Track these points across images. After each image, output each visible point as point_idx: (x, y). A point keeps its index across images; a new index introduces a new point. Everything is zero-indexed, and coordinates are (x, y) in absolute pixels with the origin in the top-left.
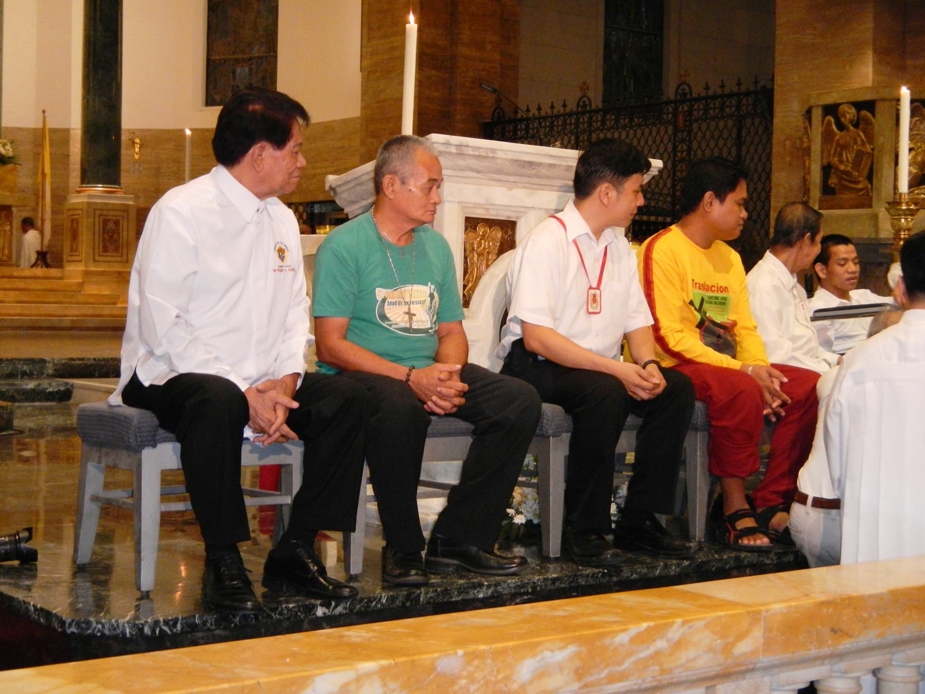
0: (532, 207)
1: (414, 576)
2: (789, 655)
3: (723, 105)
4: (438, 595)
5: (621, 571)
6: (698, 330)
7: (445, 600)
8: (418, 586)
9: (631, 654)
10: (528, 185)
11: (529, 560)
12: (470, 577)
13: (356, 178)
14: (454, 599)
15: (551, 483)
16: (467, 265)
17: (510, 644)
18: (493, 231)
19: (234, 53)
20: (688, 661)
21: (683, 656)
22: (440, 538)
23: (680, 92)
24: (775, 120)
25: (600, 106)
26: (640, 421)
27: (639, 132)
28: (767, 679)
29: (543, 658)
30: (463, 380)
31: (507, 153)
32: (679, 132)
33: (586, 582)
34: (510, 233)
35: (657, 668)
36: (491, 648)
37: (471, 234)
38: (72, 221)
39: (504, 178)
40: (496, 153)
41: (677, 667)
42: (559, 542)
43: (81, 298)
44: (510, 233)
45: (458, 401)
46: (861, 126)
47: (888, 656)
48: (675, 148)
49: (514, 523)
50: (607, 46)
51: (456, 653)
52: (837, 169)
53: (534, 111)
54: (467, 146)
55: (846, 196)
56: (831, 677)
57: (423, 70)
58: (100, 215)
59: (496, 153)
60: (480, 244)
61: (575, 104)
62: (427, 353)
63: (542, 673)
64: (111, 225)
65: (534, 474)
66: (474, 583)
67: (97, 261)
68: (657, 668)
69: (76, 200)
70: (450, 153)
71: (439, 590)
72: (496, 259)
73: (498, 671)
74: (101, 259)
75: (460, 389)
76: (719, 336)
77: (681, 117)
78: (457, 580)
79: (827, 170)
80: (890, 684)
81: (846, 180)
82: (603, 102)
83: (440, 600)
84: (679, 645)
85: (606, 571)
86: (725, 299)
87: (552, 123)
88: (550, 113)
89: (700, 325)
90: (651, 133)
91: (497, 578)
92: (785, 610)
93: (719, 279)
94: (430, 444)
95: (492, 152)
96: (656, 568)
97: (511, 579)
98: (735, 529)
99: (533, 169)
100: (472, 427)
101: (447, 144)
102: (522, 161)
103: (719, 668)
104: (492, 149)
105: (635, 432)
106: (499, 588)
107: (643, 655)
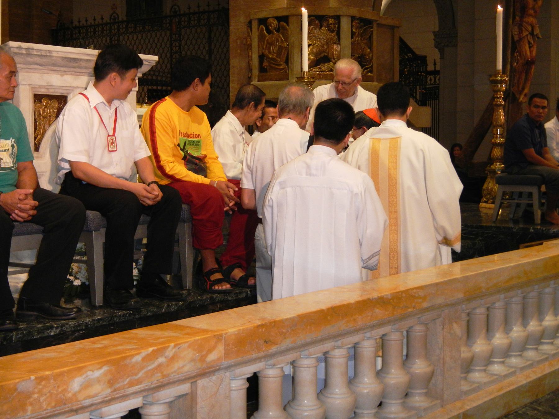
0: (77, 87)
1: (8, 325)
2: (240, 359)
4: (24, 336)
5: (141, 311)
6: (183, 161)
7: (29, 338)
8: (11, 331)
9: (143, 368)
10: (74, 73)
11: (83, 309)
12: (45, 322)
14: (35, 338)
15: (95, 260)
17: (65, 369)
18: (52, 102)
20: (179, 368)
21: (176, 366)
22: (24, 299)
23: (173, 10)
24: (231, 28)
25: (125, 19)
26: (148, 218)
27: (149, 35)
28: (227, 374)
29: (87, 376)
30: (34, 200)
33: (119, 319)
35: (158, 376)
36: (53, 373)
37: (38, 105)
39: (58, 69)
40: (52, 53)
41: (172, 373)
42: (102, 296)
45: (31, 212)
46: (281, 31)
47: (298, 353)
48: (171, 45)
49: (74, 285)
51: (30, 378)
52: (268, 57)
53: (83, 22)
54: (33, 49)
55: (273, 73)
56: (266, 368)
59: (52, 53)
60: (44, 111)
62: (11, 182)
63: (87, 385)
65: (84, 254)
66: (48, 326)
68: (159, 374)
70: (22, 54)
71: (25, 332)
72: (55, 120)
73: (58, 387)
75: (33, 205)
76: (196, 164)
77: (174, 26)
78: (36, 325)
79: (262, 57)
80: (300, 368)
81: (274, 64)
82: (127, 16)
83: (25, 338)
84: (173, 359)
85: (131, 312)
86: (199, 142)
87: (95, 29)
89: (184, 158)
91: (62, 322)
92: (236, 333)
93: (194, 129)
94: (15, 241)
95: (49, 53)
96: (162, 308)
97: (70, 321)
98: (210, 280)
100: (41, 228)
101: (20, 48)
103: (198, 371)
104: (49, 51)
105: (146, 226)
106: (64, 328)
107: (150, 368)
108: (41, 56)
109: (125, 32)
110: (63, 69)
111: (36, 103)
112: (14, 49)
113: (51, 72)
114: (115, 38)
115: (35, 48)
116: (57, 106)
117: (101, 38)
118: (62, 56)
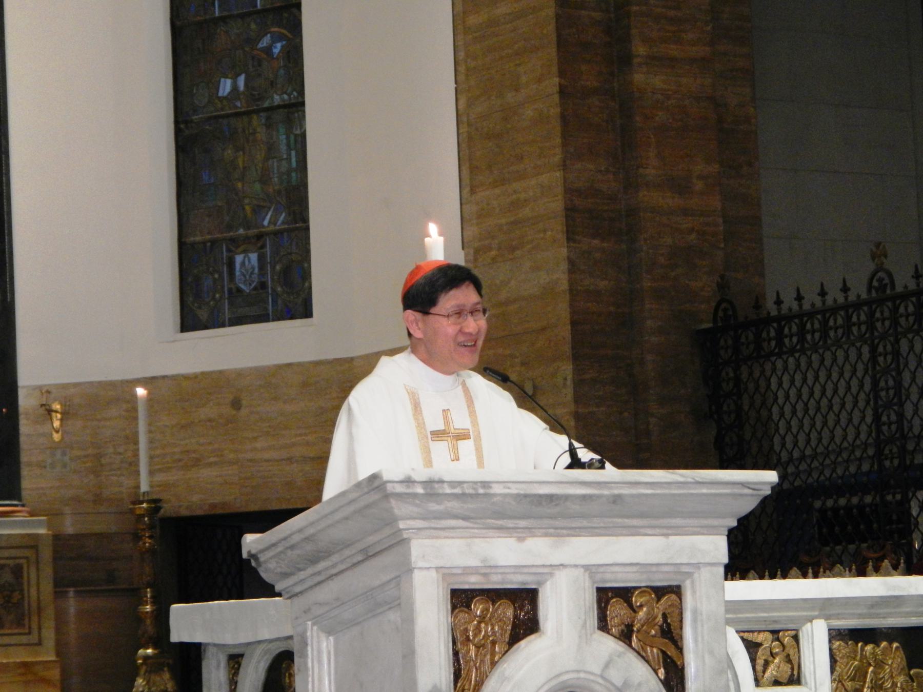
0: (562, 565)
10: (552, 531)
13: (285, 539)
16: (459, 664)
19: (230, 227)
31: (510, 485)
34: (527, 607)
37: (461, 615)
39: (510, 523)
40: (491, 487)
44: (527, 607)
53: (789, 302)
54: (441, 482)
57: (575, 241)
59: (491, 487)
60: (478, 629)
61: (865, 281)
70: (415, 495)
72: (506, 652)
87: (825, 322)
99: (556, 505)
102: (535, 495)
104: (481, 482)
108: (462, 497)
109: (915, 327)
110: (522, 523)
111: (457, 611)
112: (396, 485)
113: (491, 533)
114: (885, 347)
115: (446, 479)
116: (511, 617)
117: (833, 349)
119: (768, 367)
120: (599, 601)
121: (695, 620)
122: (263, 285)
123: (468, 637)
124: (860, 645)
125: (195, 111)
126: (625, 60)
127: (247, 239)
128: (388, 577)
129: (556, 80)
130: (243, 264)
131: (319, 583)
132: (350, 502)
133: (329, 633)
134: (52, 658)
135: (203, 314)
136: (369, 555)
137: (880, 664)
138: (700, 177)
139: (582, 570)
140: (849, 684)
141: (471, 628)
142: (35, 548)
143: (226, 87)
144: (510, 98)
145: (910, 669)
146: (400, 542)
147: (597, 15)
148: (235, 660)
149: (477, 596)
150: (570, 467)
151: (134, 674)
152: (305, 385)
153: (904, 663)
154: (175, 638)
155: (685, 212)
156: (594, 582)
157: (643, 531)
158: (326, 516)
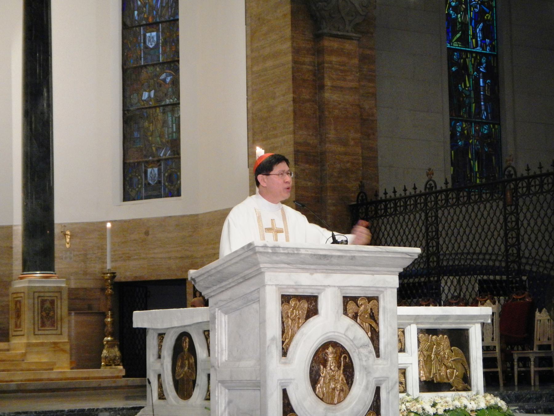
0: (329, 286)
3: (542, 183)
10: (325, 271)
13: (208, 272)
16: (284, 327)
19: (146, 156)
31: (308, 250)
32: (508, 206)
34: (314, 304)
37: (286, 306)
38: (16, 302)
39: (307, 267)
43: (24, 366)
44: (314, 304)
48: (505, 219)
50: (453, 136)
53: (390, 194)
54: (279, 247)
57: (298, 165)
58: (39, 297)
60: (292, 312)
61: (423, 186)
64: (47, 305)
67: (38, 335)
69: (19, 285)
70: (268, 253)
72: (304, 323)
74: (40, 332)
77: (508, 194)
88: (403, 195)
90: (479, 209)
95: (297, 250)
99: (327, 259)
102: (319, 255)
104: (296, 248)
108: (287, 254)
110: (313, 267)
113: (299, 270)
114: (432, 214)
116: (307, 307)
118: (310, 253)
119: (380, 221)
120: (344, 302)
121: (384, 312)
122: (159, 182)
123: (288, 315)
124: (430, 336)
125: (132, 105)
126: (321, 87)
127: (153, 162)
128: (254, 289)
129: (291, 95)
130: (151, 173)
131: (223, 291)
132: (238, 256)
133: (226, 313)
134: (67, 341)
135: (133, 194)
136: (246, 279)
137: (439, 344)
138: (353, 139)
139: (337, 288)
140: (425, 353)
141: (289, 312)
142: (60, 292)
143: (145, 95)
144: (271, 102)
145: (451, 347)
146: (260, 273)
147: (310, 68)
148: (161, 336)
149: (292, 298)
150: (333, 243)
151: (102, 347)
152: (177, 225)
153: (449, 344)
154: (135, 325)
155: (345, 154)
156: (342, 294)
157: (363, 272)
158: (227, 262)
